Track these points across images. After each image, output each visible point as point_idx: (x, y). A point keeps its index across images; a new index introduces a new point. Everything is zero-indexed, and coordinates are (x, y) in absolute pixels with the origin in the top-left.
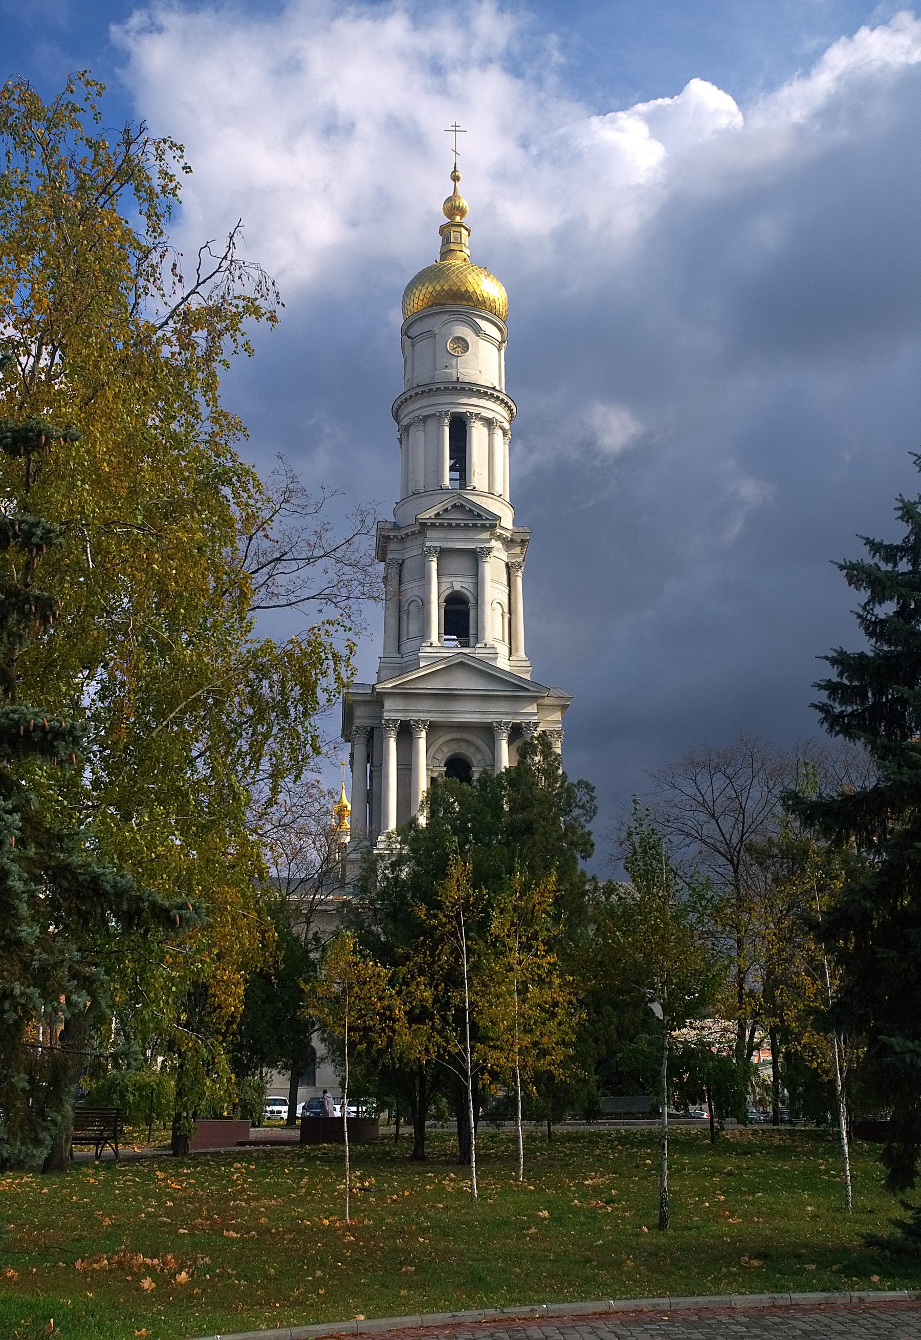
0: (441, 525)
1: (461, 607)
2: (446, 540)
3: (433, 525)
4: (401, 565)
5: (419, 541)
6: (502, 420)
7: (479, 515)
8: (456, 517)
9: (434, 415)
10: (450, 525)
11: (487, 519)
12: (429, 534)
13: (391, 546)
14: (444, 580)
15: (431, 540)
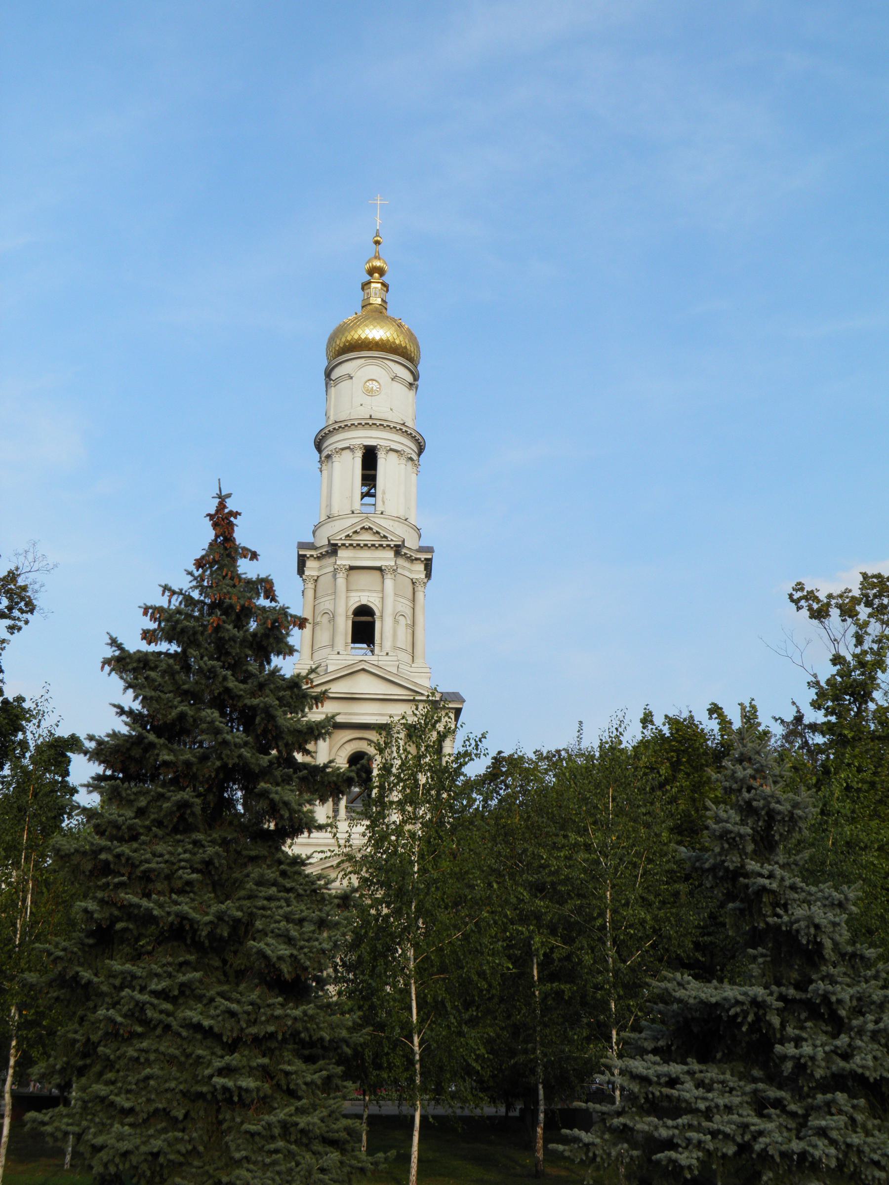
0: (351, 545)
1: (369, 619)
2: (355, 558)
3: (343, 545)
4: (316, 581)
5: (331, 560)
6: (410, 451)
7: (385, 537)
8: (366, 537)
9: (348, 448)
10: (358, 545)
11: (392, 540)
12: (341, 553)
13: (310, 564)
14: (352, 594)
15: (342, 559)
